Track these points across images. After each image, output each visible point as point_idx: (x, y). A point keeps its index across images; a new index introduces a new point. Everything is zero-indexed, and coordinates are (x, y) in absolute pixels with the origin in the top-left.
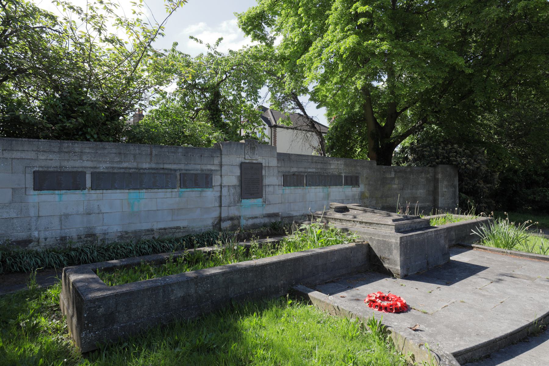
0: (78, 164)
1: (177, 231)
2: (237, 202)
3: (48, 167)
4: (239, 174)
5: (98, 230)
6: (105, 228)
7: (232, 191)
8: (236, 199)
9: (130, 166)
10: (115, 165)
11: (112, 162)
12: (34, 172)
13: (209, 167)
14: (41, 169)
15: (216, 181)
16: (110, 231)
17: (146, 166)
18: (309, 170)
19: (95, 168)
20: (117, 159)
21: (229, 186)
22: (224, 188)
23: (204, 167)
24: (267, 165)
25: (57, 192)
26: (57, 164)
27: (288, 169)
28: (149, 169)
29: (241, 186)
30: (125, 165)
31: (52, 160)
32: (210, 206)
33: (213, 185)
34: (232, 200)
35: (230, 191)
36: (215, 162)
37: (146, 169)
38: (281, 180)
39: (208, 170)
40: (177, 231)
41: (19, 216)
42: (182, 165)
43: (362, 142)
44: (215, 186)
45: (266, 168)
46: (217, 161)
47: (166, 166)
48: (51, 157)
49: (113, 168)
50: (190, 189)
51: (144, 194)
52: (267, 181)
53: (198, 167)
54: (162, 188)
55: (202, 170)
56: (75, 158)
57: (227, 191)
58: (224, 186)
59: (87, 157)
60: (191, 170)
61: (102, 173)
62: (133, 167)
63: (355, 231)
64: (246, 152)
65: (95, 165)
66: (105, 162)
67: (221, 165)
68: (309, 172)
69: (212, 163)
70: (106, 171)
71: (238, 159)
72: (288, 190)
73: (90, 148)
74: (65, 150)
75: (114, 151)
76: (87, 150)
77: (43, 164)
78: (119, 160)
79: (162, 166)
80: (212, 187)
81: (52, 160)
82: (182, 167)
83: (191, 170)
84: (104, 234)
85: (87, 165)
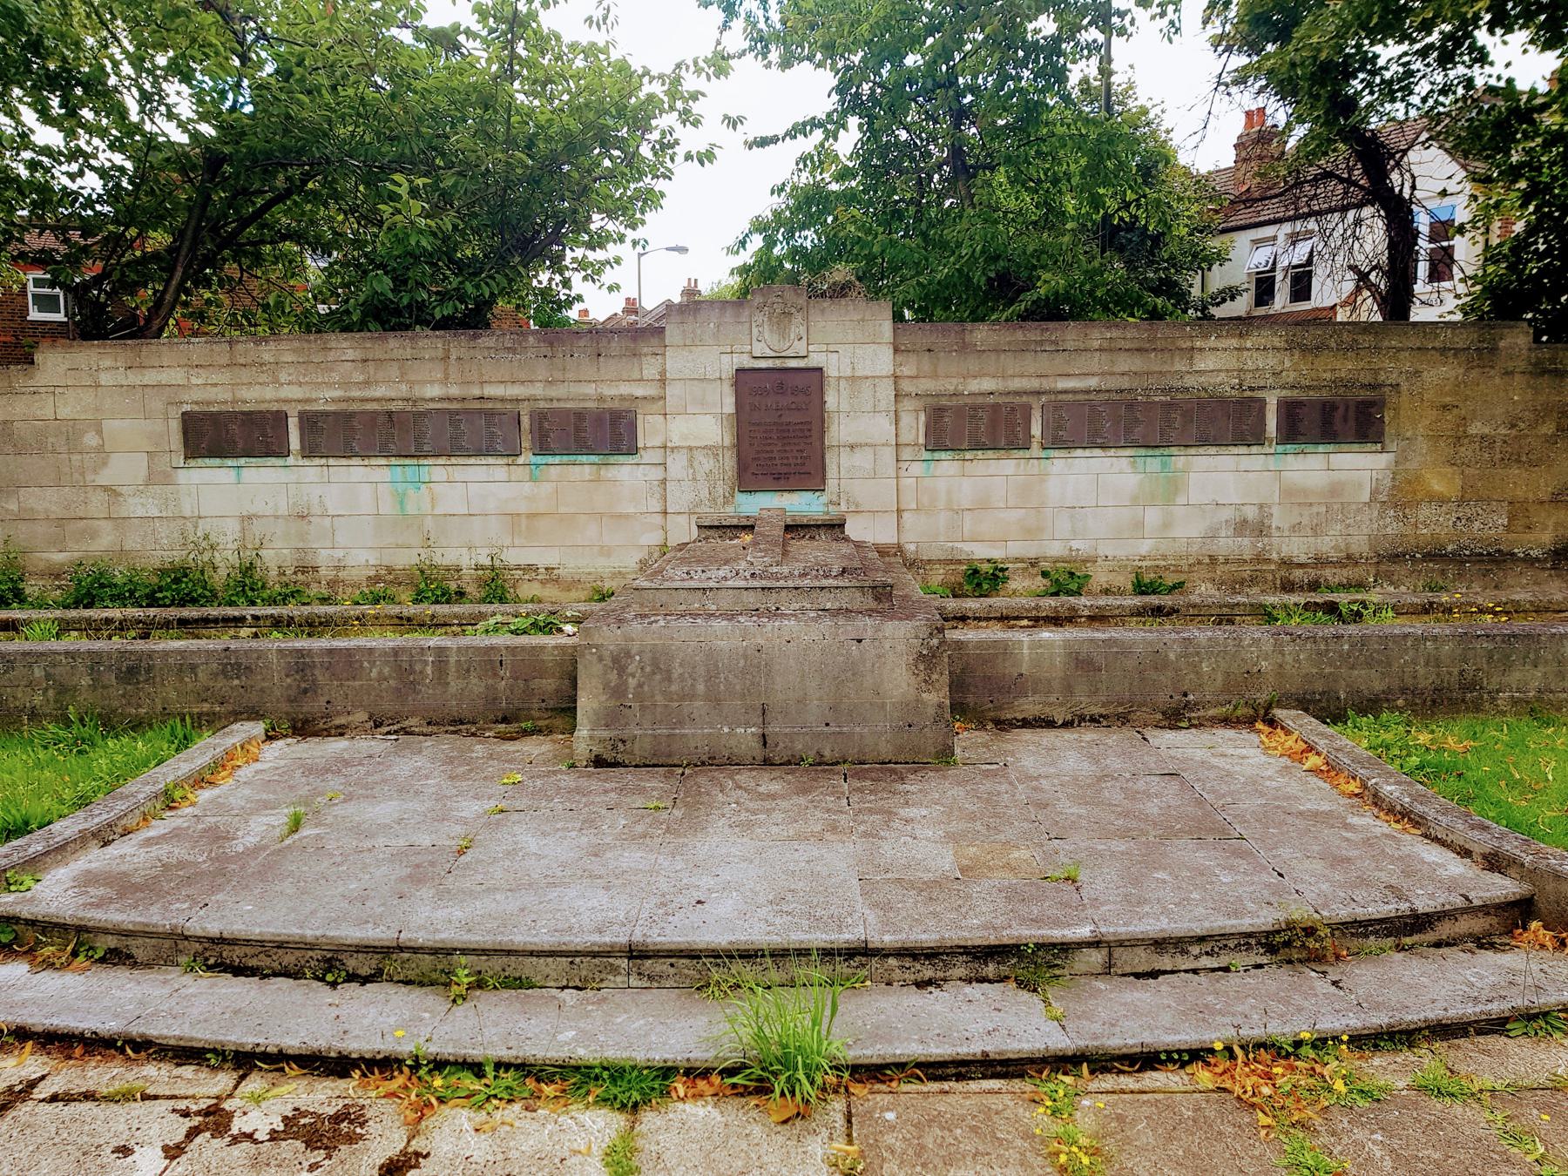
0: (269, 393)
1: (527, 577)
2: (721, 500)
3: (209, 403)
4: (730, 407)
5: (324, 558)
6: (340, 553)
7: (706, 464)
8: (721, 489)
9: (393, 394)
10: (356, 393)
11: (346, 384)
12: (183, 414)
13: (625, 389)
14: (196, 408)
15: (650, 430)
16: (349, 562)
17: (433, 391)
18: (1062, 384)
19: (308, 401)
20: (359, 377)
21: (690, 449)
22: (675, 455)
23: (609, 391)
24: (849, 373)
25: (229, 462)
26: (228, 396)
27: (950, 385)
28: (441, 399)
29: (739, 446)
30: (379, 392)
31: (215, 385)
32: (632, 510)
33: (640, 445)
34: (705, 494)
35: (696, 464)
36: (645, 372)
37: (432, 400)
38: (914, 426)
39: (623, 398)
40: (527, 577)
41: (164, 514)
42: (538, 384)
43: (336, 262)
44: (645, 448)
45: (843, 383)
46: (650, 369)
47: (489, 391)
48: (215, 378)
49: (347, 400)
50: (565, 459)
51: (436, 471)
52: (840, 430)
53: (590, 389)
54: (479, 453)
55: (601, 399)
56: (264, 378)
57: (685, 463)
58: (673, 449)
59: (290, 375)
60: (568, 399)
61: (326, 414)
62: (400, 395)
63: (714, 1069)
64: (755, 331)
65: (308, 395)
66: (329, 385)
67: (663, 381)
68: (1065, 392)
69: (636, 375)
70: (331, 408)
71: (726, 359)
72: (947, 465)
73: (294, 351)
74: (242, 361)
75: (350, 355)
76: (289, 357)
77: (197, 395)
78: (361, 378)
79: (476, 392)
80: (633, 450)
81: (215, 385)
82: (538, 390)
83: (568, 399)
84: (337, 568)
85: (290, 396)
